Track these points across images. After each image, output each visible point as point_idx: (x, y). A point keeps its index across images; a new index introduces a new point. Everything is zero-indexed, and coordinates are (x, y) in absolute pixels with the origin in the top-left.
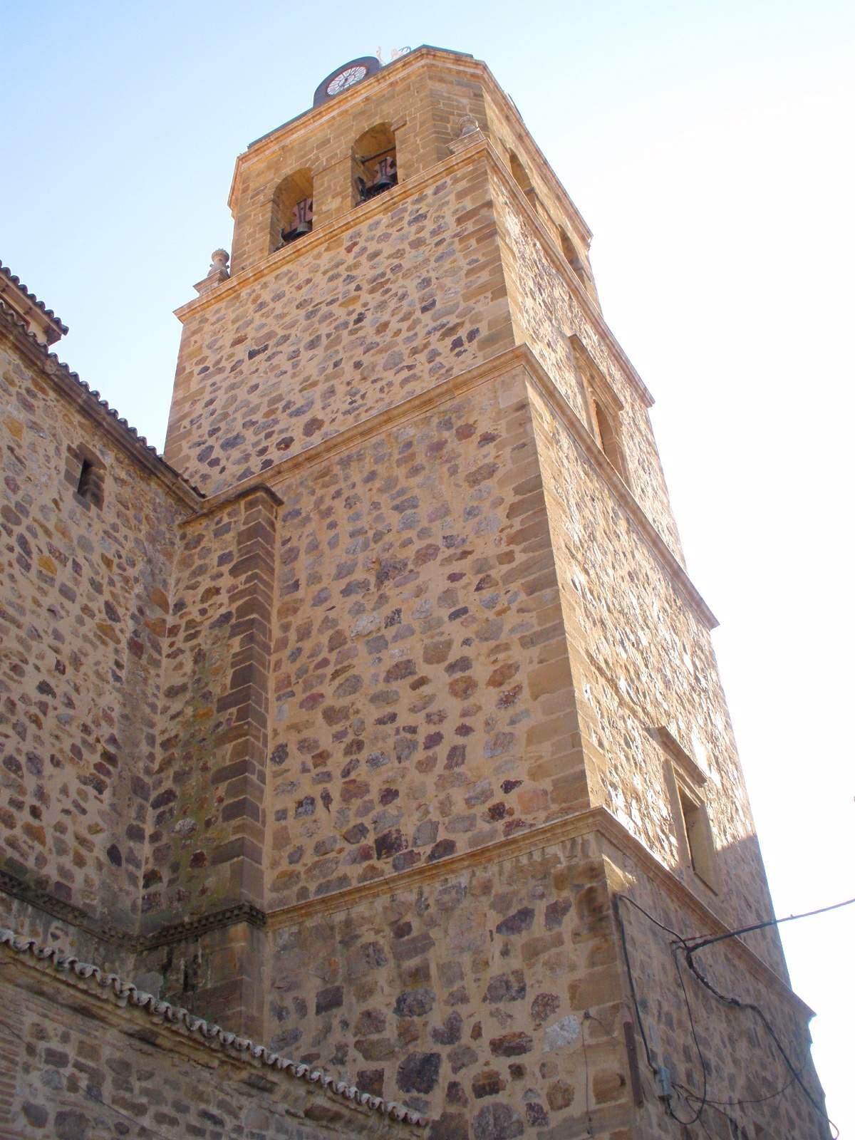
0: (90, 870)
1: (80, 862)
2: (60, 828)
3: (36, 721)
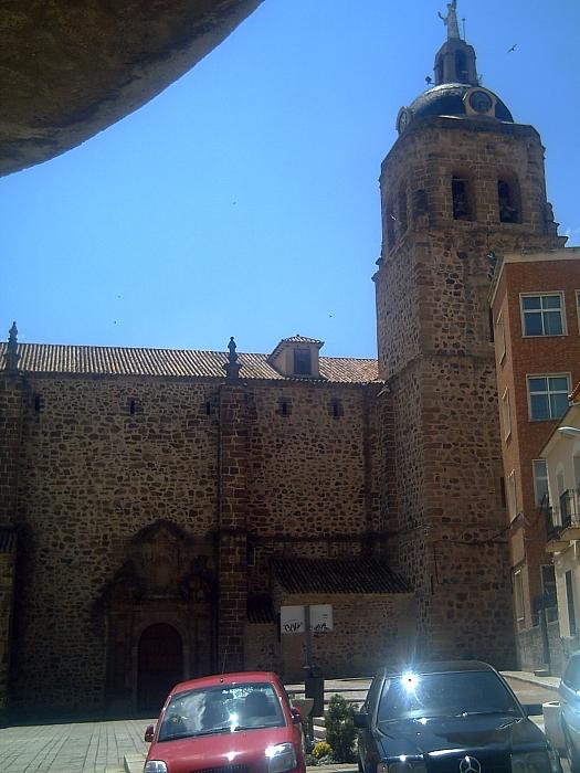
0: (362, 525)
1: (358, 525)
2: (350, 519)
3: (337, 494)
